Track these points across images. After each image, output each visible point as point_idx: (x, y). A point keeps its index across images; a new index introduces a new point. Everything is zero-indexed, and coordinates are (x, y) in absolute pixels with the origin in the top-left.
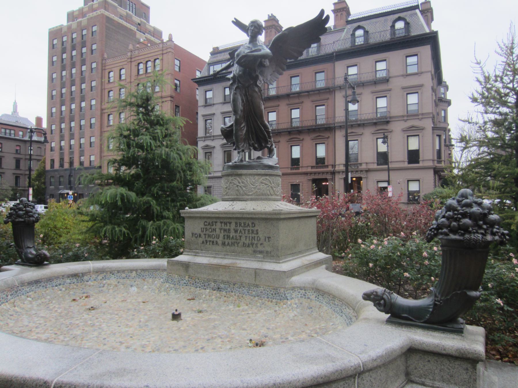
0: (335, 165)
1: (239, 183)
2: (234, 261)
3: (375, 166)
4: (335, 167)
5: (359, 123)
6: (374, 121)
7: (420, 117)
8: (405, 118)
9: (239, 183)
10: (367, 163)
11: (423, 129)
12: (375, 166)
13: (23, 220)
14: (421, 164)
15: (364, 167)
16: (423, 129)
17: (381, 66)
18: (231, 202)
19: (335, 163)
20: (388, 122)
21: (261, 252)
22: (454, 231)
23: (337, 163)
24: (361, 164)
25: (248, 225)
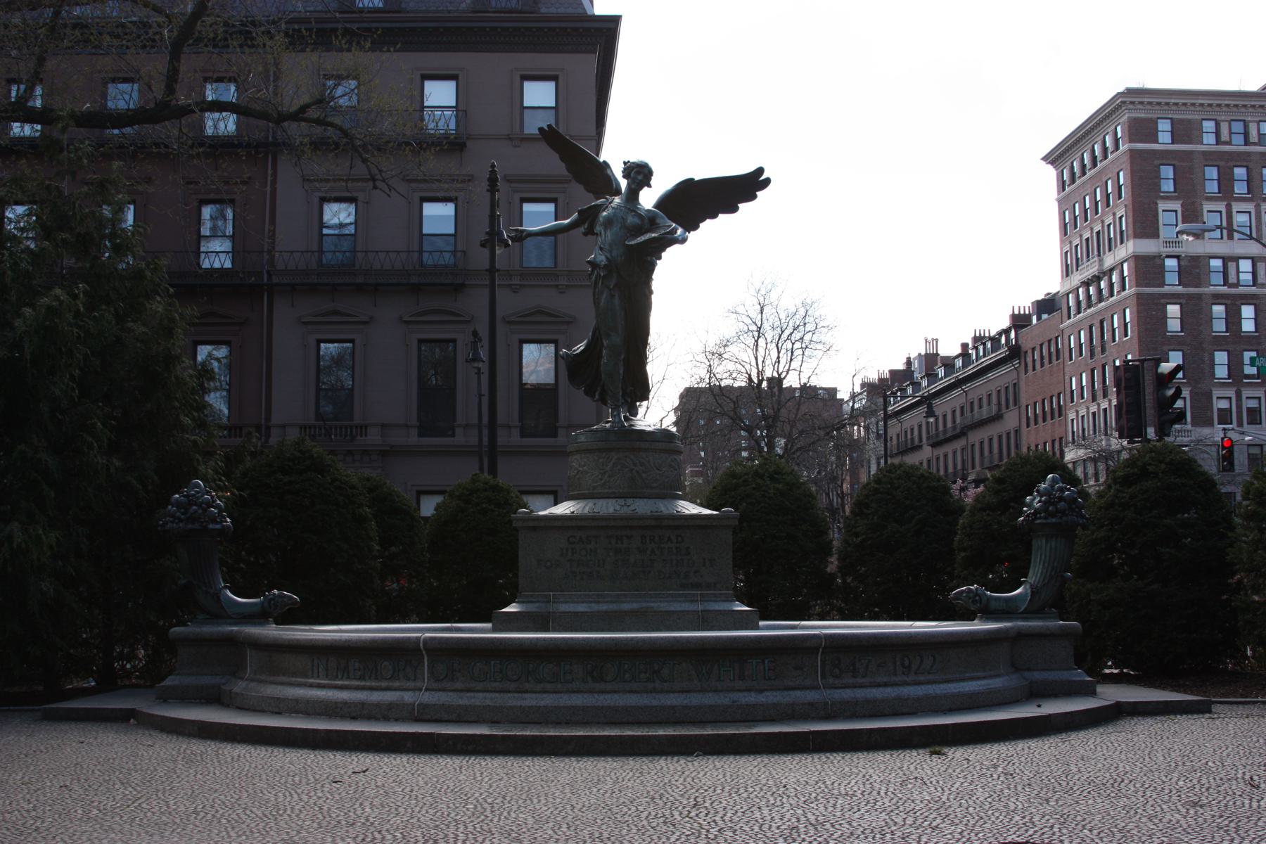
0: (268, 428)
1: (635, 464)
2: (644, 605)
3: (413, 439)
4: (268, 436)
5: (360, 280)
6: (414, 280)
7: (563, 281)
8: (516, 281)
9: (635, 464)
10: (383, 426)
11: (569, 323)
12: (413, 439)
13: (218, 526)
14: (561, 439)
15: (374, 437)
16: (569, 323)
17: (440, 94)
18: (621, 501)
19: (268, 419)
20: (458, 288)
21: (696, 586)
22: (1052, 515)
23: (276, 419)
24: (363, 428)
25: (669, 539)
